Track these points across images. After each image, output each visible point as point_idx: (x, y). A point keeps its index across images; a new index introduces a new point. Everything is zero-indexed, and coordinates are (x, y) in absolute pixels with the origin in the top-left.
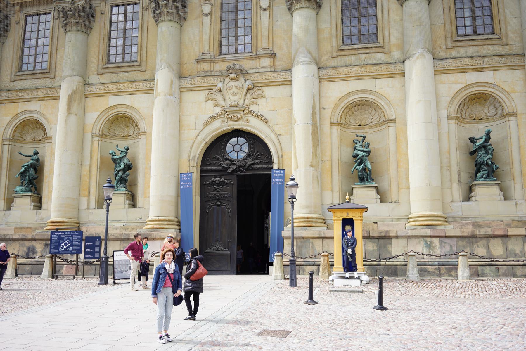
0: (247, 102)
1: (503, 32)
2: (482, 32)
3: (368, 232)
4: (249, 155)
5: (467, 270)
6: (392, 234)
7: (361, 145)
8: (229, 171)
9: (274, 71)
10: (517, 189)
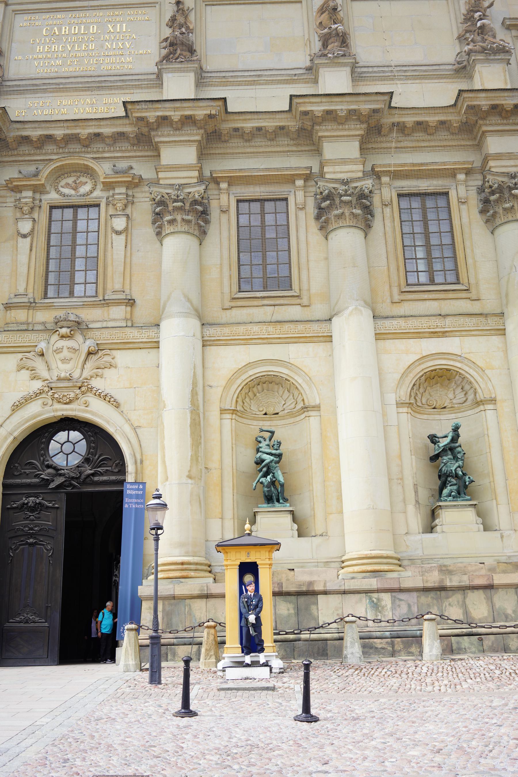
0: (86, 374)
1: (472, 281)
2: (443, 281)
3: (280, 585)
4: (87, 460)
5: (437, 644)
6: (319, 587)
7: (268, 445)
8: (52, 486)
9: (132, 326)
10: (501, 515)
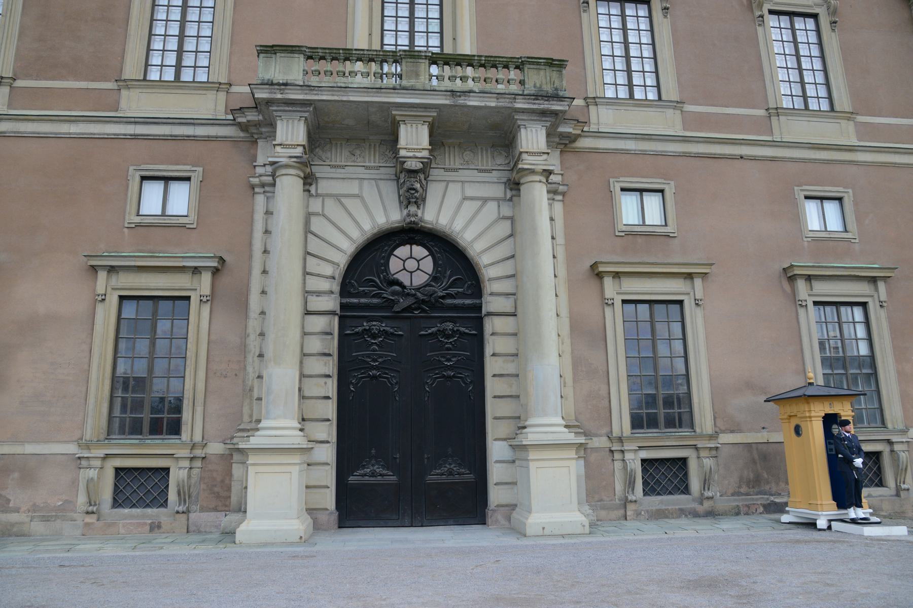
8: (397, 308)
